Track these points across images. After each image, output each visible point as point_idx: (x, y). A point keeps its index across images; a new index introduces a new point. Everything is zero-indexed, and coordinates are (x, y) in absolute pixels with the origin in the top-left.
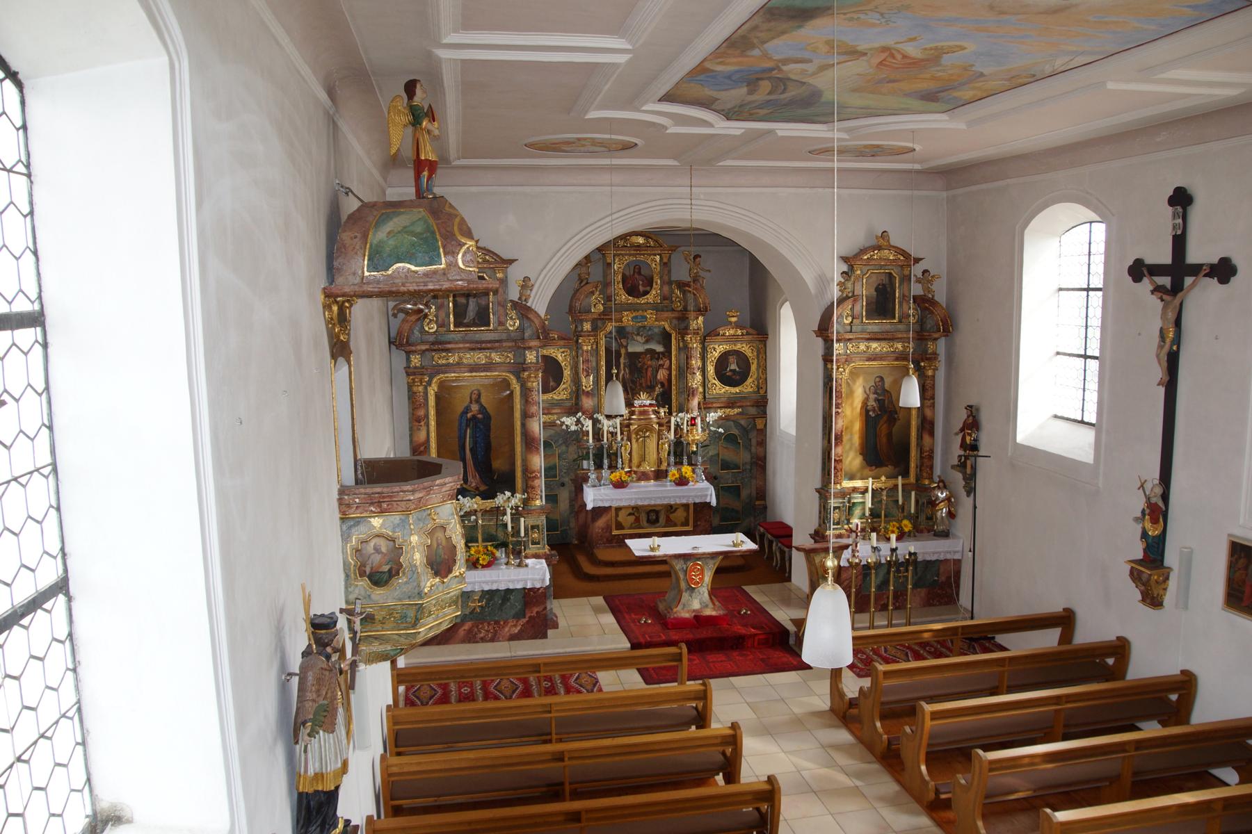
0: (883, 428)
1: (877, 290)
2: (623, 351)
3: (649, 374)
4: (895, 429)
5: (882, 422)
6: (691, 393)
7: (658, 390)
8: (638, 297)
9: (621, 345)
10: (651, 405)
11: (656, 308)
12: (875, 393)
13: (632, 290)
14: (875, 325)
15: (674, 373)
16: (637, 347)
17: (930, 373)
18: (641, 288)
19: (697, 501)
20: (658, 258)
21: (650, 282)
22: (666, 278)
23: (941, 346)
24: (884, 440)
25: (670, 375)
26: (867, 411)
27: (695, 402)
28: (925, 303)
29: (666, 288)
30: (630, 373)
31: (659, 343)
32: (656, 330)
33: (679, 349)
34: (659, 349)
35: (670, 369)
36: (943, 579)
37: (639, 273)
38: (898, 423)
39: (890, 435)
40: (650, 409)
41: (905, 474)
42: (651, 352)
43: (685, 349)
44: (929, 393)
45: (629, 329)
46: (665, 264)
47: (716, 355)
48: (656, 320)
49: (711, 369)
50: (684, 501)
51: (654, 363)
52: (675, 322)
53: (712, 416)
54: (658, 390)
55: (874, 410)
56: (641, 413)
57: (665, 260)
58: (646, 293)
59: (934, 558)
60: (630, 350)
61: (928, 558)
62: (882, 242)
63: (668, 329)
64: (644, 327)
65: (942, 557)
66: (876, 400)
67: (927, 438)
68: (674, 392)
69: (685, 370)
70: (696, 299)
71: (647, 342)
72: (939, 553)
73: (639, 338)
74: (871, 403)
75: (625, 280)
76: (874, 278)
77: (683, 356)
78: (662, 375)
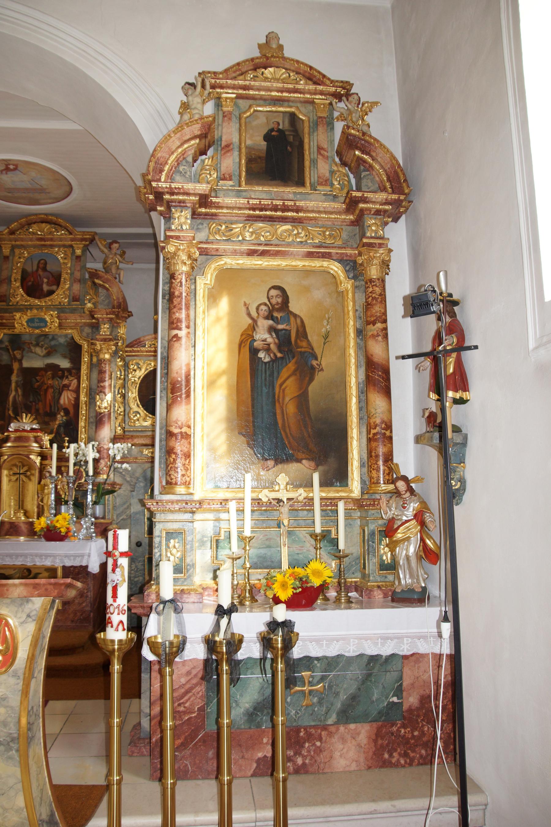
0: (288, 387)
1: (267, 137)
2: (16, 366)
3: (49, 396)
4: (313, 388)
5: (285, 373)
6: (98, 420)
7: (61, 418)
8: (39, 298)
9: (15, 358)
10: (33, 430)
11: (61, 309)
12: (270, 316)
13: (33, 289)
14: (264, 193)
15: (83, 398)
16: (35, 361)
17: (374, 272)
18: (45, 288)
19: (68, 563)
20: (69, 251)
21: (56, 280)
22: (78, 275)
23: (397, 234)
24: (291, 409)
25: (77, 399)
26: (254, 352)
27: (106, 432)
28: (356, 147)
29: (77, 287)
30: (24, 395)
31: (65, 357)
32: (62, 340)
33: (91, 366)
34: (65, 364)
35: (77, 391)
36: (412, 700)
37: (45, 269)
38: (319, 377)
39: (302, 399)
40: (31, 435)
41: (338, 476)
42: (54, 368)
43: (98, 366)
44: (377, 309)
45: (26, 338)
46: (78, 257)
47: (141, 373)
48: (60, 326)
49: (133, 394)
50: (48, 563)
51: (56, 383)
52: (87, 330)
53: (117, 450)
54: (61, 418)
55: (268, 350)
56: (18, 439)
57: (78, 252)
58: (51, 293)
59: (386, 651)
60: (26, 364)
61: (372, 651)
62: (269, 55)
63: (77, 338)
64: (46, 335)
65: (405, 650)
66: (271, 329)
67: (377, 401)
68: (82, 424)
69: (96, 391)
70: (109, 295)
71: (48, 354)
72: (400, 638)
73: (38, 350)
74: (262, 335)
75: (25, 276)
76: (262, 120)
77: (95, 375)
78: (66, 398)
